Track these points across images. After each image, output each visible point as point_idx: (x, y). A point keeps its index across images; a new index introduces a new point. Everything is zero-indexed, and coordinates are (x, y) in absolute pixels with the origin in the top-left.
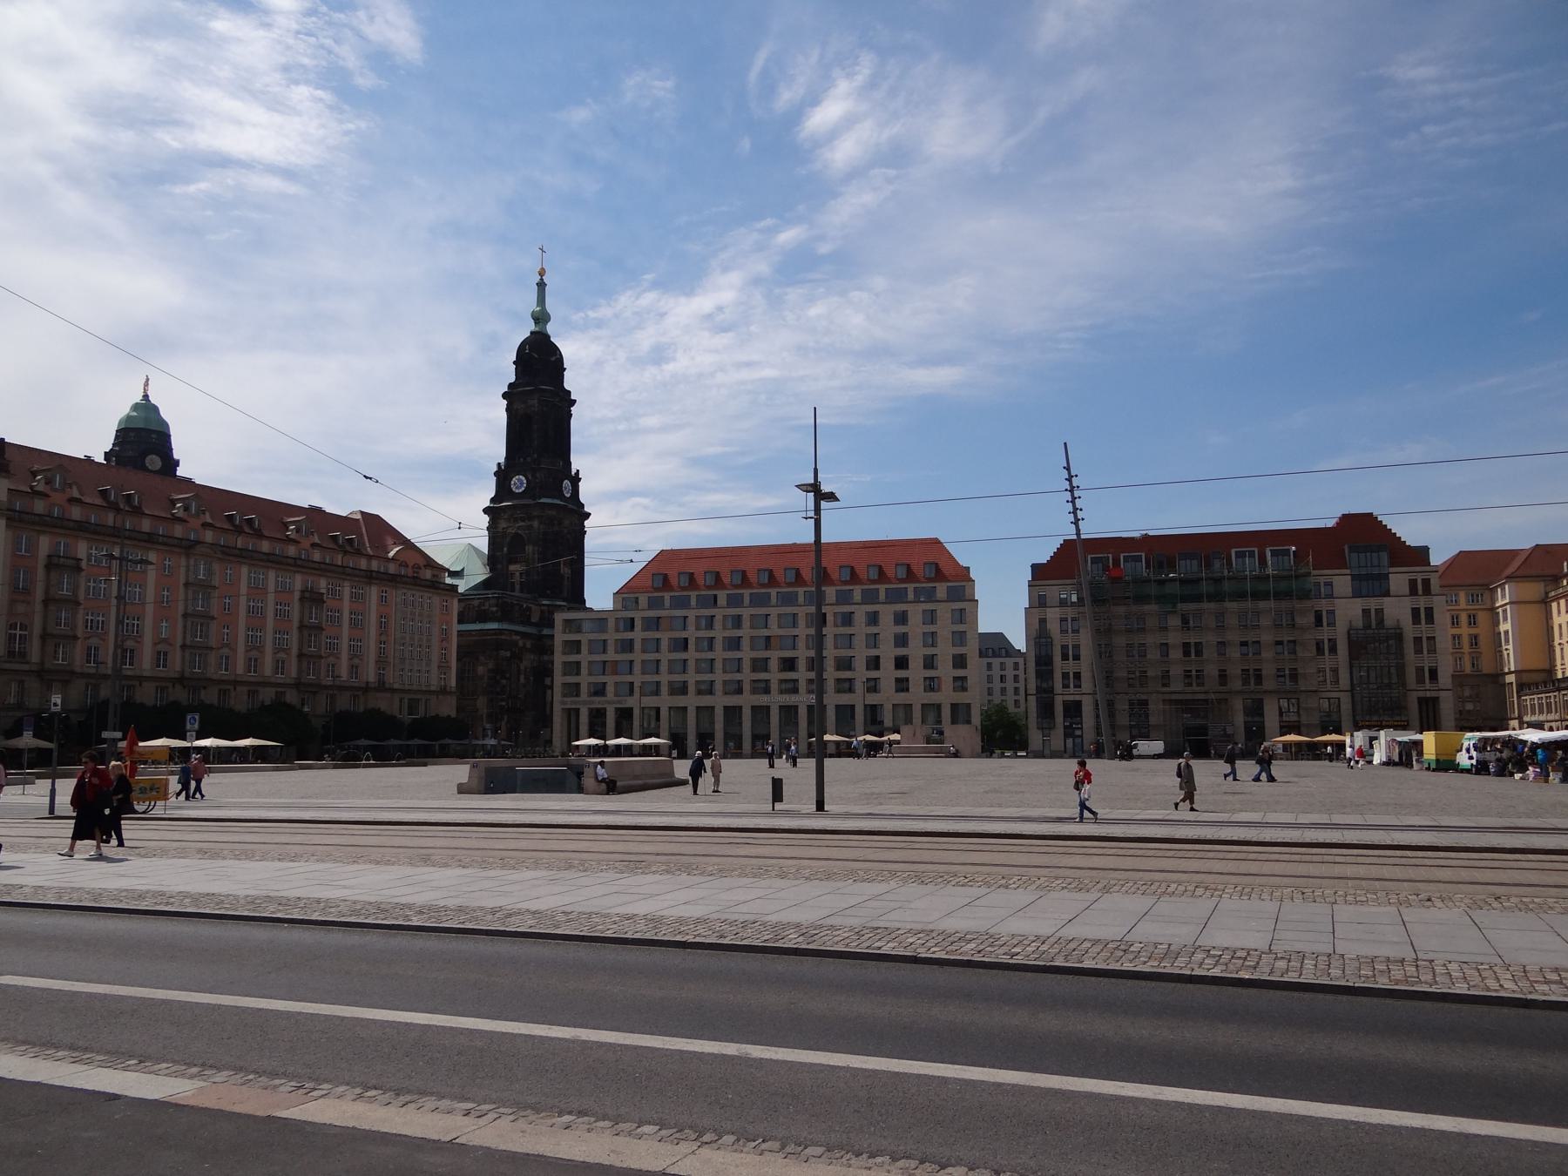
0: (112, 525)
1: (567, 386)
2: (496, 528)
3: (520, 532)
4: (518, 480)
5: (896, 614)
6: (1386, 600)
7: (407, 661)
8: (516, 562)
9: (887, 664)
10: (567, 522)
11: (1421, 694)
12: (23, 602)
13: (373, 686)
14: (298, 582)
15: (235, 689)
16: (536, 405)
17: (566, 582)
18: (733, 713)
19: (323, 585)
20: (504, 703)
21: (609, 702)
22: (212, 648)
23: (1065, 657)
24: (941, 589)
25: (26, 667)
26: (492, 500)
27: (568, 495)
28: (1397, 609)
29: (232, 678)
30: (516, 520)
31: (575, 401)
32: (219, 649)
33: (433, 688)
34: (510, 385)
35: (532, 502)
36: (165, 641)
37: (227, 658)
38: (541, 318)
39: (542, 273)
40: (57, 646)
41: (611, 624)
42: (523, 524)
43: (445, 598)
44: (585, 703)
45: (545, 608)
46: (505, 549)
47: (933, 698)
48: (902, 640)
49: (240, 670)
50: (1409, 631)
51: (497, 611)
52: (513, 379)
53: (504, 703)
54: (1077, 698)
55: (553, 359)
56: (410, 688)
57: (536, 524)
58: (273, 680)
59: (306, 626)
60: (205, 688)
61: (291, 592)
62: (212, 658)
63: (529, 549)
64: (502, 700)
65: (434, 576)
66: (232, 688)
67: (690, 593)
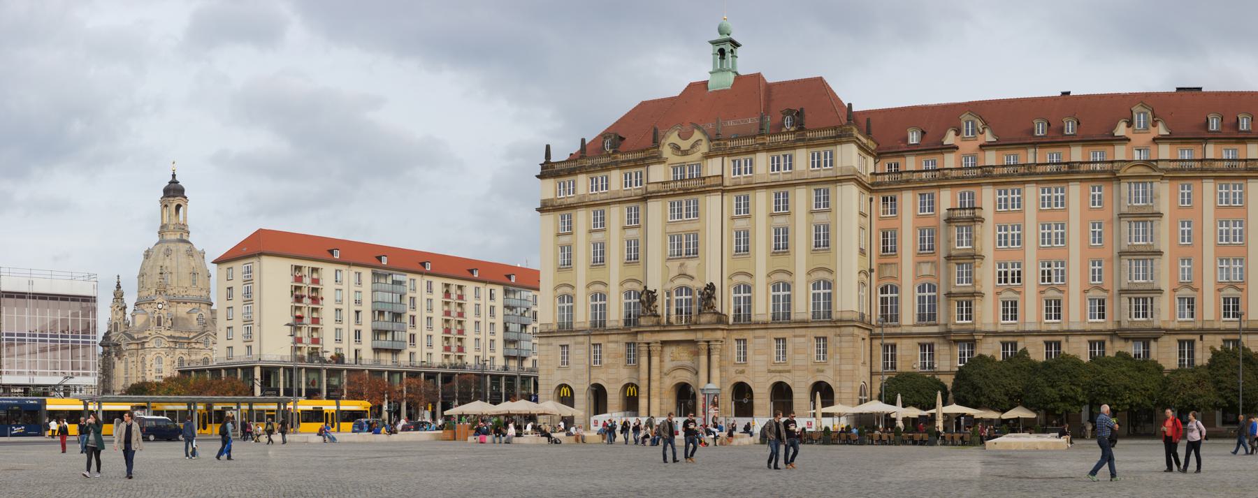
0: (1139, 159)
15: (1201, 339)
25: (935, 329)
29: (1199, 325)
66: (1197, 338)
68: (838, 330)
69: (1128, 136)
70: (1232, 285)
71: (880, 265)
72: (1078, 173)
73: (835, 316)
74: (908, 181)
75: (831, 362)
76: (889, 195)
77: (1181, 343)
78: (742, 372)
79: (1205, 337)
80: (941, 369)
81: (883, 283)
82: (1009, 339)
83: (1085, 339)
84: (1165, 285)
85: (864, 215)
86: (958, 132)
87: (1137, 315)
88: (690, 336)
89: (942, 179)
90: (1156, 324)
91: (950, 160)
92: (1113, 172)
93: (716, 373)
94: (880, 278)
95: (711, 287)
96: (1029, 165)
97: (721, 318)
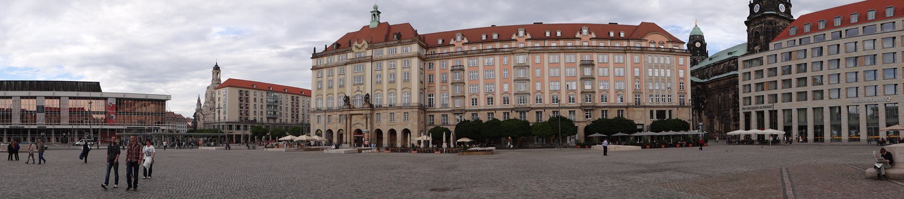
13: (631, 105)
18: (761, 126)
21: (766, 107)
29: (543, 106)
33: (674, 104)
36: (506, 93)
44: (753, 108)
56: (658, 105)
58: (567, 106)
60: (528, 111)
69: (516, 39)
71: (429, 87)
74: (437, 57)
76: (431, 62)
77: (537, 112)
78: (379, 125)
79: (546, 110)
80: (450, 124)
81: (429, 93)
82: (475, 113)
83: (502, 112)
84: (531, 93)
85: (422, 69)
86: (455, 40)
87: (521, 103)
88: (360, 112)
89: (451, 56)
90: (528, 106)
91: (452, 49)
92: (511, 52)
93: (369, 125)
94: (428, 92)
95: (368, 94)
96: (480, 50)
97: (371, 106)
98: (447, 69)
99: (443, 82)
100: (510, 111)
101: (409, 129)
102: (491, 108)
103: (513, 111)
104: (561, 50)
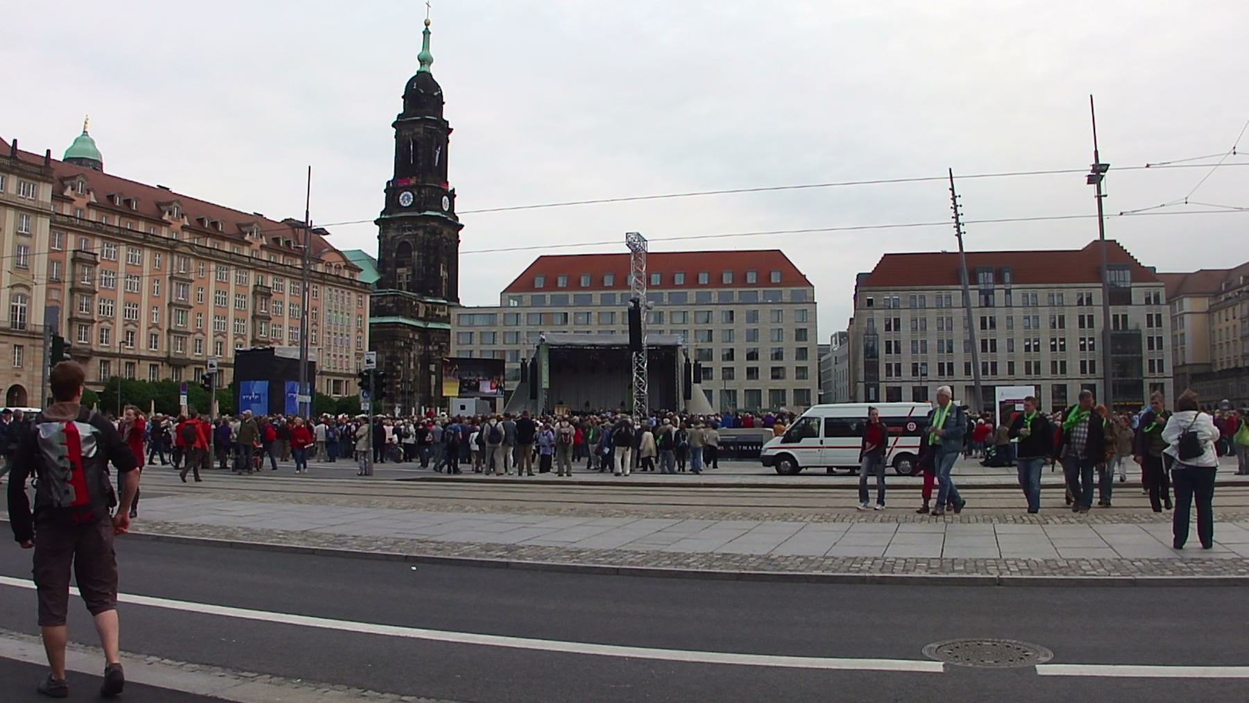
1: (445, 117)
2: (386, 236)
3: (406, 240)
4: (408, 195)
5: (748, 313)
6: (1129, 307)
7: (332, 348)
8: (403, 266)
9: (740, 356)
10: (445, 233)
11: (1152, 381)
12: (56, 289)
14: (252, 278)
16: (422, 132)
17: (444, 284)
19: (270, 281)
20: (399, 386)
22: (189, 333)
23: (888, 351)
24: (786, 293)
26: (382, 213)
27: (446, 209)
28: (1136, 315)
30: (404, 230)
31: (452, 129)
32: (194, 334)
33: (351, 372)
34: (399, 116)
35: (418, 214)
36: (156, 326)
37: (221, 343)
38: (425, 60)
39: (427, 24)
40: (80, 327)
41: (500, 317)
42: (410, 233)
43: (360, 294)
45: (428, 305)
46: (394, 255)
47: (778, 384)
48: (753, 335)
49: (210, 353)
50: (1145, 332)
51: (392, 308)
52: (401, 111)
53: (399, 386)
54: (898, 385)
55: (436, 94)
56: (334, 371)
57: (421, 233)
59: (259, 316)
61: (247, 287)
62: (190, 341)
63: (415, 254)
64: (398, 383)
65: (353, 275)
67: (569, 293)
68: (32, 342)
69: (171, 221)
70: (221, 334)
72: (149, 242)
73: (29, 328)
75: (26, 368)
83: (149, 363)
98: (64, 251)
99: (51, 281)
100: (160, 363)
101: (25, 386)
102: (131, 352)
103: (165, 364)
104: (233, 260)
